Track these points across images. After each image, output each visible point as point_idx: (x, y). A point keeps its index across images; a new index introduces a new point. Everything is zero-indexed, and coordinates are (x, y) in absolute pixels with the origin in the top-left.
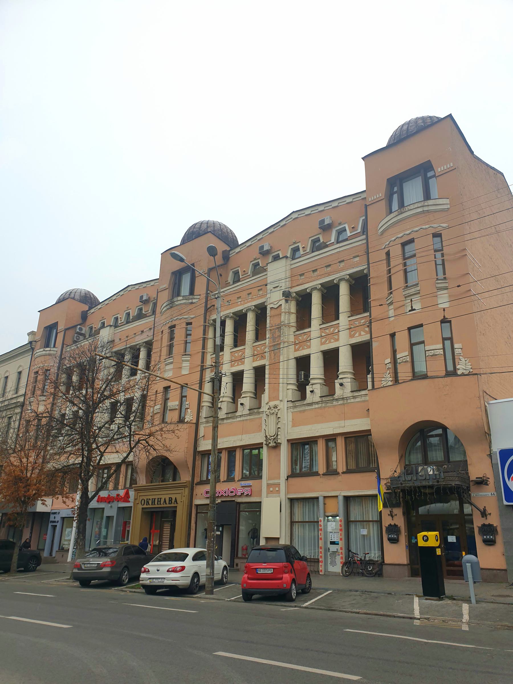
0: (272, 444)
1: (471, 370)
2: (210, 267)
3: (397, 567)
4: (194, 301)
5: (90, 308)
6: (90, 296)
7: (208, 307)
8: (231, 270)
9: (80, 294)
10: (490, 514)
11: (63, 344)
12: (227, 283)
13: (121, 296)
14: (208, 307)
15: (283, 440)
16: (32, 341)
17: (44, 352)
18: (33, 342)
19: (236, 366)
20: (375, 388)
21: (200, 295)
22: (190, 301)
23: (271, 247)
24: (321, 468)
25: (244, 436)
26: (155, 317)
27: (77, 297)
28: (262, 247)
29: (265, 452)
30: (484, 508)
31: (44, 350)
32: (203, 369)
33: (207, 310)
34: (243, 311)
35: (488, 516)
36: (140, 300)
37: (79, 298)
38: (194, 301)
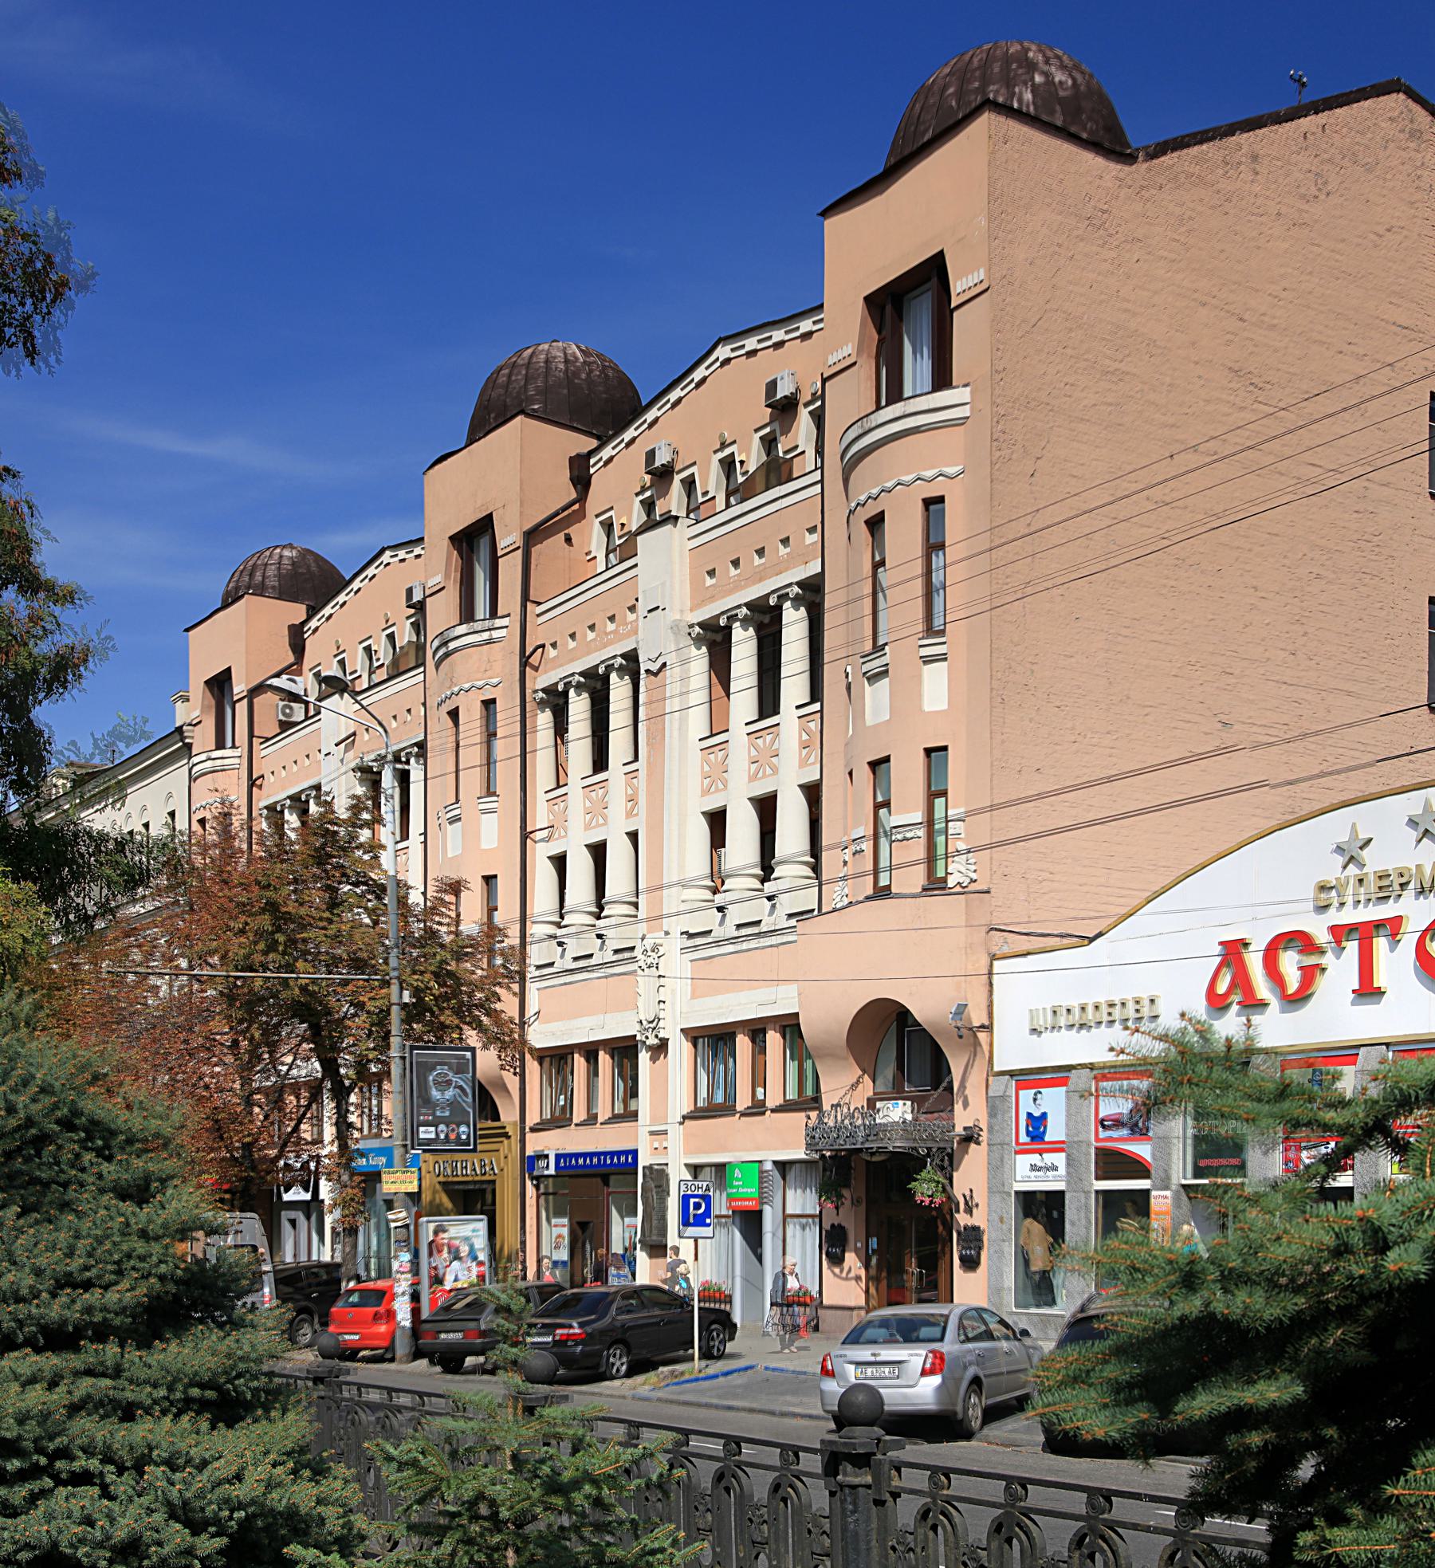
0: (652, 1041)
1: (974, 876)
2: (527, 526)
3: (839, 1312)
4: (495, 634)
5: (312, 612)
6: (309, 567)
7: (527, 654)
8: (597, 516)
9: (279, 569)
10: (977, 1205)
11: (251, 735)
12: (588, 558)
13: (371, 579)
14: (527, 654)
15: (671, 1030)
16: (181, 727)
17: (209, 764)
18: (185, 728)
19: (594, 827)
20: (824, 911)
21: (508, 615)
22: (485, 636)
23: (675, 452)
24: (743, 1102)
25: (608, 1016)
26: (424, 672)
27: (272, 582)
28: (651, 455)
29: (644, 1057)
30: (968, 1193)
31: (209, 759)
32: (525, 836)
33: (525, 661)
34: (600, 672)
35: (975, 1210)
36: (408, 601)
37: (277, 584)
38: (495, 634)
